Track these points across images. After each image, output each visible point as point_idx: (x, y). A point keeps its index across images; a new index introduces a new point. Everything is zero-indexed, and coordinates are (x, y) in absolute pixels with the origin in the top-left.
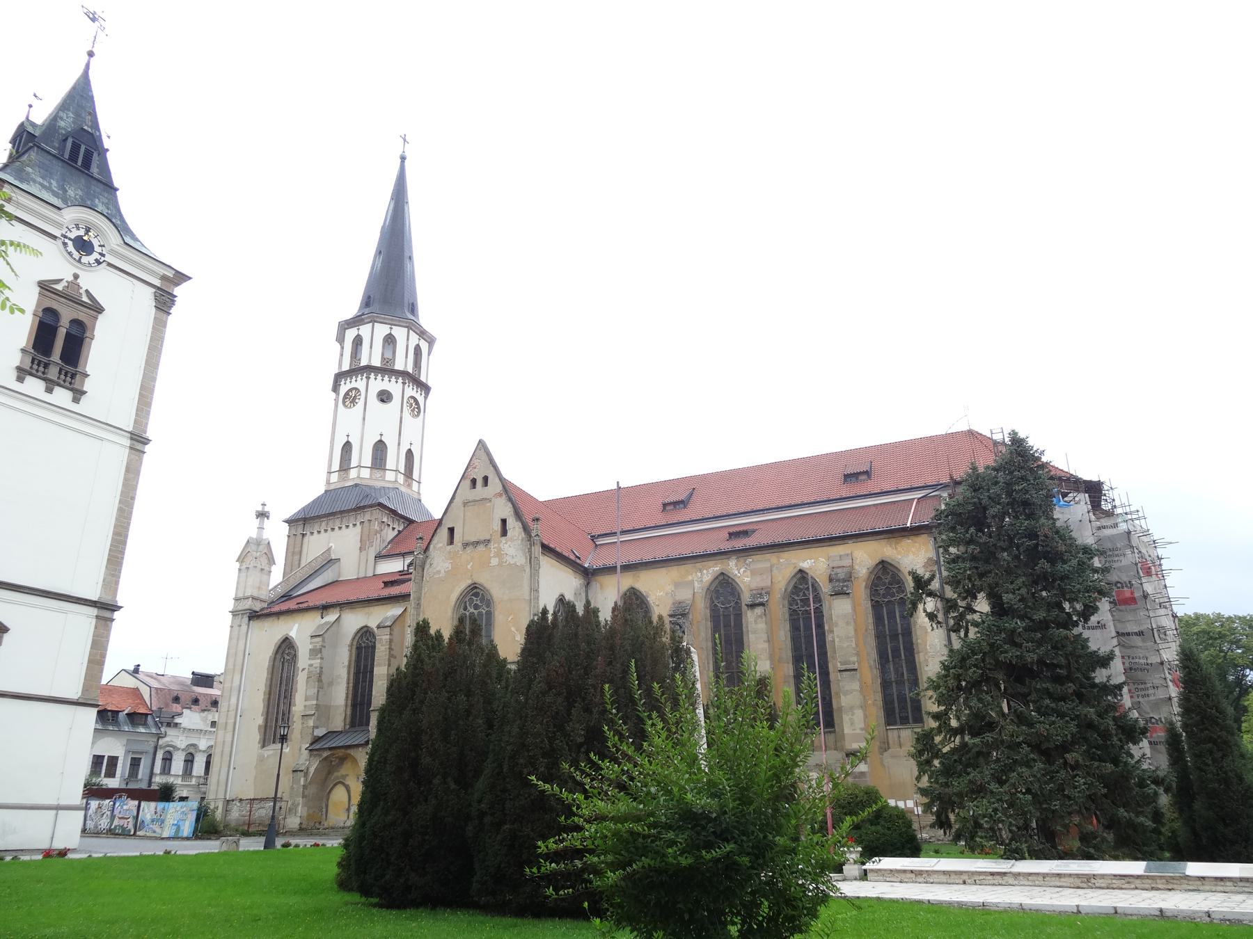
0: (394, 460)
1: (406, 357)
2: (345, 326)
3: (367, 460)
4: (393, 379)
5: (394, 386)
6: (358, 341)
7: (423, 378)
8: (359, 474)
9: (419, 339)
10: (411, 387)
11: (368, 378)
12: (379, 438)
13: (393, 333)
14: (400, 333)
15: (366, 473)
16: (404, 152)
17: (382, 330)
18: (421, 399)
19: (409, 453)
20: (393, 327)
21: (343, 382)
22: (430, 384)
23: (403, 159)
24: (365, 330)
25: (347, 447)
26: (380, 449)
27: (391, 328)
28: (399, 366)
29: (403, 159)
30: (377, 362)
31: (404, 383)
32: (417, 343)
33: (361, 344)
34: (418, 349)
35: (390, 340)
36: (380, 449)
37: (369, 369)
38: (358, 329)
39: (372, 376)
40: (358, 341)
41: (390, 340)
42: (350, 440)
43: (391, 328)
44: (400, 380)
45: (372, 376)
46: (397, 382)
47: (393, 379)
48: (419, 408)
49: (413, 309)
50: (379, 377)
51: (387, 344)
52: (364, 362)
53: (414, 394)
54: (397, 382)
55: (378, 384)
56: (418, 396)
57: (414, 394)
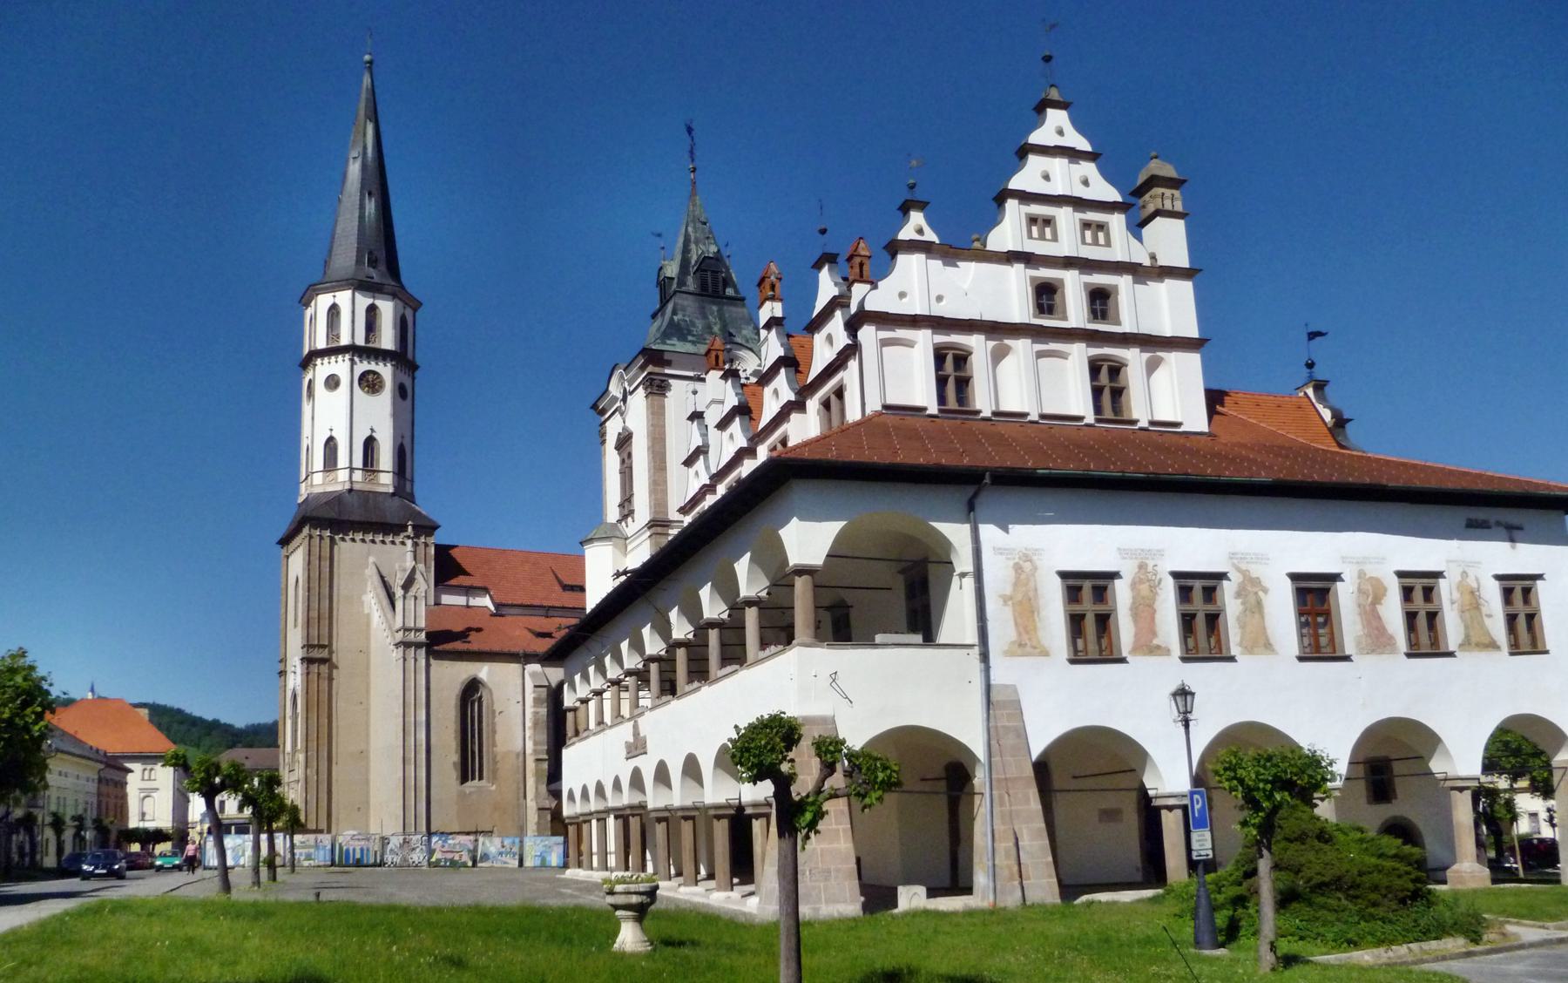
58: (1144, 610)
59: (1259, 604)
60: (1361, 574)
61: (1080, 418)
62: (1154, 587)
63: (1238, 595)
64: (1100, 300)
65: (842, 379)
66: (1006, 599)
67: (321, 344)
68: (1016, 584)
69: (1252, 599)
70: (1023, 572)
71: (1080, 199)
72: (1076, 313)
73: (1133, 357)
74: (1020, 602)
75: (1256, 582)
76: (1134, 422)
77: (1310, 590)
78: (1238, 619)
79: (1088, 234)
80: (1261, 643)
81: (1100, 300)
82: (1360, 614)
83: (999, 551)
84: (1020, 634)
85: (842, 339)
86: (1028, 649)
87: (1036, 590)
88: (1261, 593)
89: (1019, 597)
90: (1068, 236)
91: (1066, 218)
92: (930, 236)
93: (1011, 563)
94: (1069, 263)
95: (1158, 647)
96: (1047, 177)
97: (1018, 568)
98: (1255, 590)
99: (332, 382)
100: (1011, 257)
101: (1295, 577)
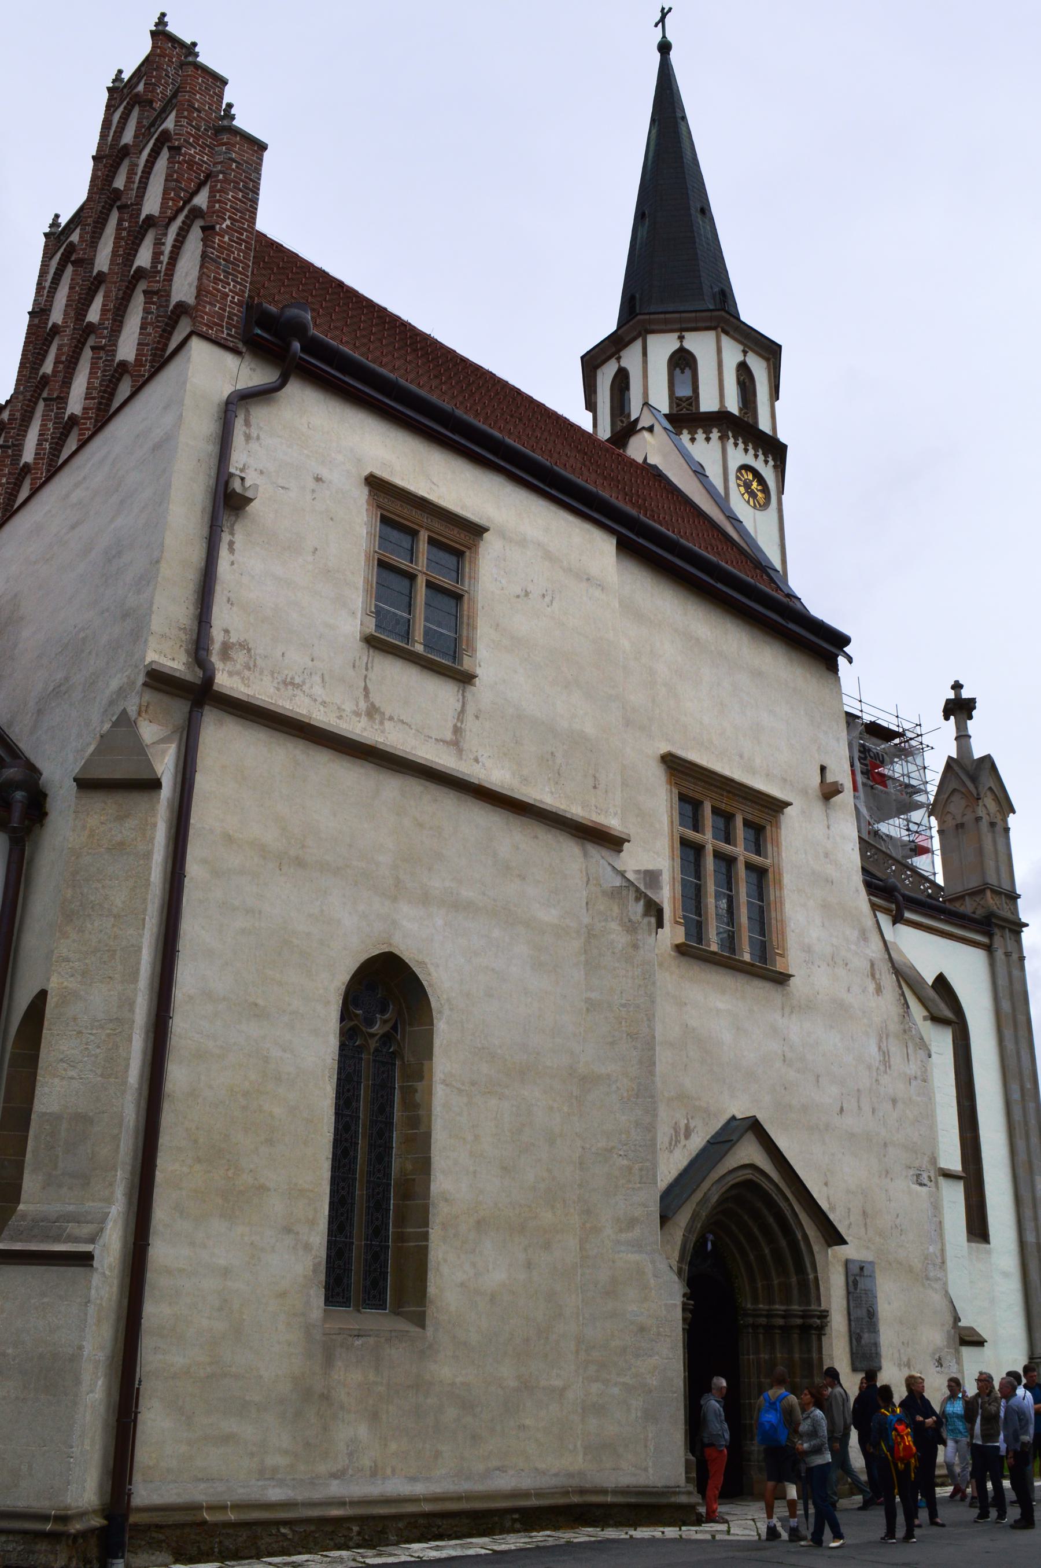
2: (591, 362)
4: (700, 436)
9: (745, 353)
10: (741, 446)
13: (687, 345)
16: (664, 36)
18: (768, 473)
20: (683, 333)
22: (782, 437)
23: (665, 48)
27: (681, 338)
28: (708, 403)
29: (665, 48)
31: (723, 438)
32: (741, 358)
33: (627, 387)
34: (743, 369)
43: (681, 338)
44: (715, 435)
46: (708, 439)
47: (700, 436)
48: (766, 490)
49: (725, 297)
51: (678, 370)
53: (749, 460)
54: (708, 439)
56: (759, 465)
57: (749, 460)
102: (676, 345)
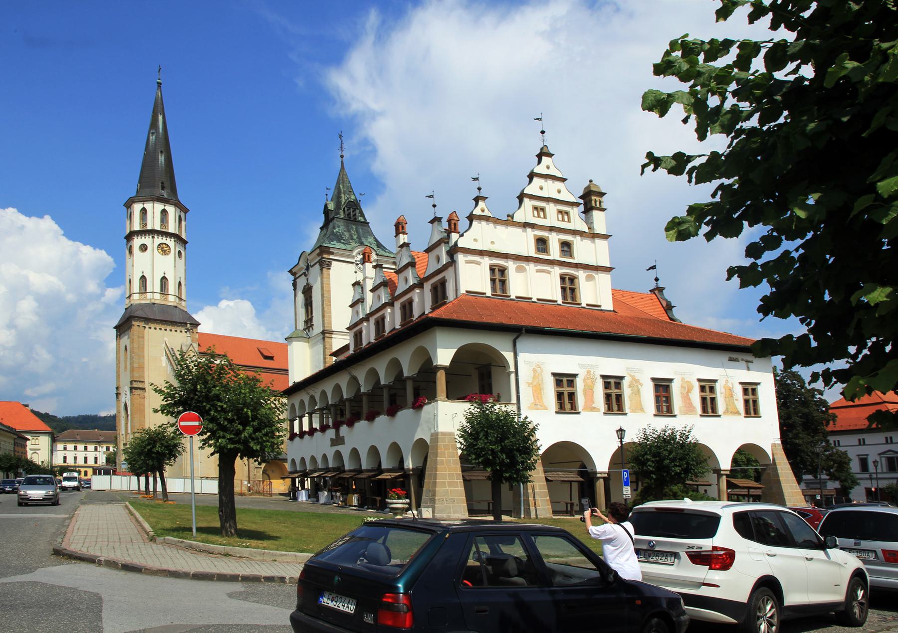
0: (172, 288)
1: (175, 222)
3: (157, 288)
5: (171, 242)
6: (144, 211)
7: (184, 236)
8: (153, 297)
11: (153, 237)
12: (163, 275)
14: (171, 209)
15: (157, 296)
17: (159, 207)
19: (180, 284)
21: (136, 238)
24: (148, 206)
25: (143, 278)
26: (164, 280)
27: (165, 206)
30: (158, 227)
35: (164, 212)
36: (164, 280)
37: (153, 232)
38: (143, 204)
39: (156, 237)
40: (144, 211)
41: (164, 212)
42: (144, 275)
44: (173, 240)
45: (156, 237)
50: (160, 238)
52: (149, 227)
55: (159, 240)
58: (589, 391)
59: (639, 391)
60: (683, 379)
61: (556, 301)
62: (593, 382)
63: (630, 386)
64: (566, 247)
65: (445, 277)
66: (529, 384)
67: (137, 227)
68: (534, 377)
69: (635, 388)
70: (537, 373)
71: (558, 200)
72: (555, 252)
73: (581, 274)
74: (535, 386)
75: (637, 381)
76: (580, 304)
77: (660, 386)
78: (629, 397)
79: (560, 216)
80: (640, 408)
81: (566, 247)
82: (682, 397)
83: (527, 363)
84: (535, 400)
85: (445, 259)
86: (539, 407)
87: (542, 380)
88: (639, 386)
89: (535, 384)
90: (552, 217)
91: (551, 209)
92: (486, 213)
93: (532, 368)
94: (552, 229)
95: (595, 408)
96: (541, 188)
97: (534, 370)
98: (637, 384)
99: (144, 248)
100: (526, 225)
101: (653, 379)
102: (163, 208)
